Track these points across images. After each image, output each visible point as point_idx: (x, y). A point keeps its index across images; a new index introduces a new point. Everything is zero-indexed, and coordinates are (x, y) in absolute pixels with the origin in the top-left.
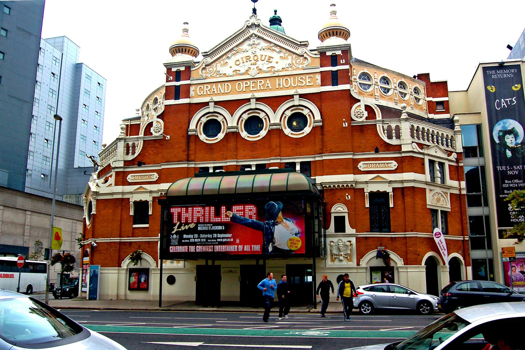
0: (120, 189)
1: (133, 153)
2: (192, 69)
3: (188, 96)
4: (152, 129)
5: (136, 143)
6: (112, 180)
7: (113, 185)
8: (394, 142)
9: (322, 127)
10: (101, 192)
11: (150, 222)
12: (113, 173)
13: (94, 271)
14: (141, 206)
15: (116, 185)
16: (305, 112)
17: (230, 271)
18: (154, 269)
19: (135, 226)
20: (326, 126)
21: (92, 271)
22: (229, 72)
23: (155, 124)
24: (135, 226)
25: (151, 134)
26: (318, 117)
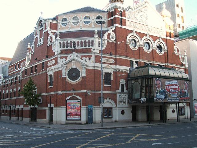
0: (98, 65)
1: (102, 47)
2: (126, 12)
3: (125, 25)
4: (110, 37)
5: (103, 42)
6: (93, 59)
7: (94, 62)
8: (184, 63)
9: (167, 53)
10: (88, 65)
11: (112, 83)
12: (93, 55)
13: (91, 108)
14: (108, 75)
15: (96, 62)
16: (162, 45)
17: (143, 108)
18: (114, 107)
19: (105, 85)
20: (168, 52)
21: (89, 108)
22: (139, 19)
23: (111, 34)
24: (105, 85)
25: (110, 39)
26: (166, 48)
